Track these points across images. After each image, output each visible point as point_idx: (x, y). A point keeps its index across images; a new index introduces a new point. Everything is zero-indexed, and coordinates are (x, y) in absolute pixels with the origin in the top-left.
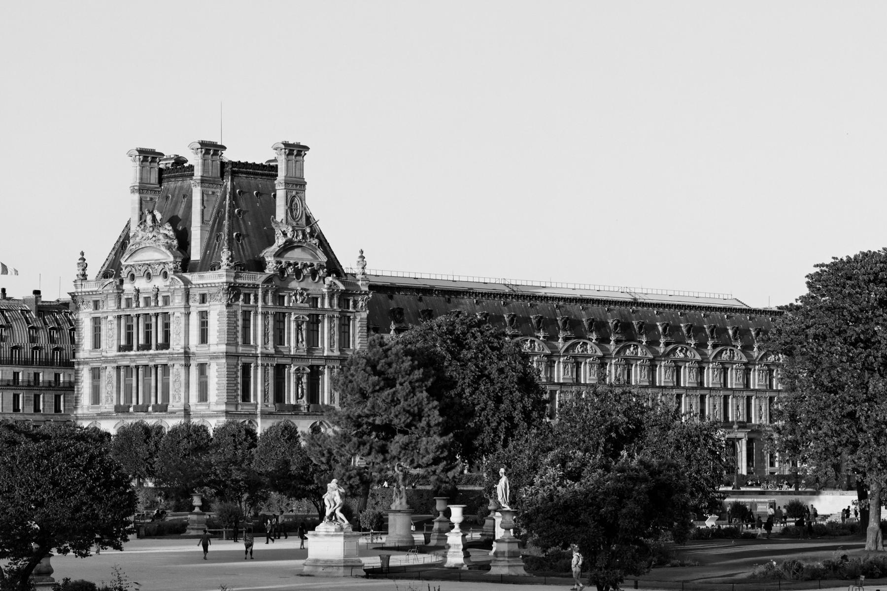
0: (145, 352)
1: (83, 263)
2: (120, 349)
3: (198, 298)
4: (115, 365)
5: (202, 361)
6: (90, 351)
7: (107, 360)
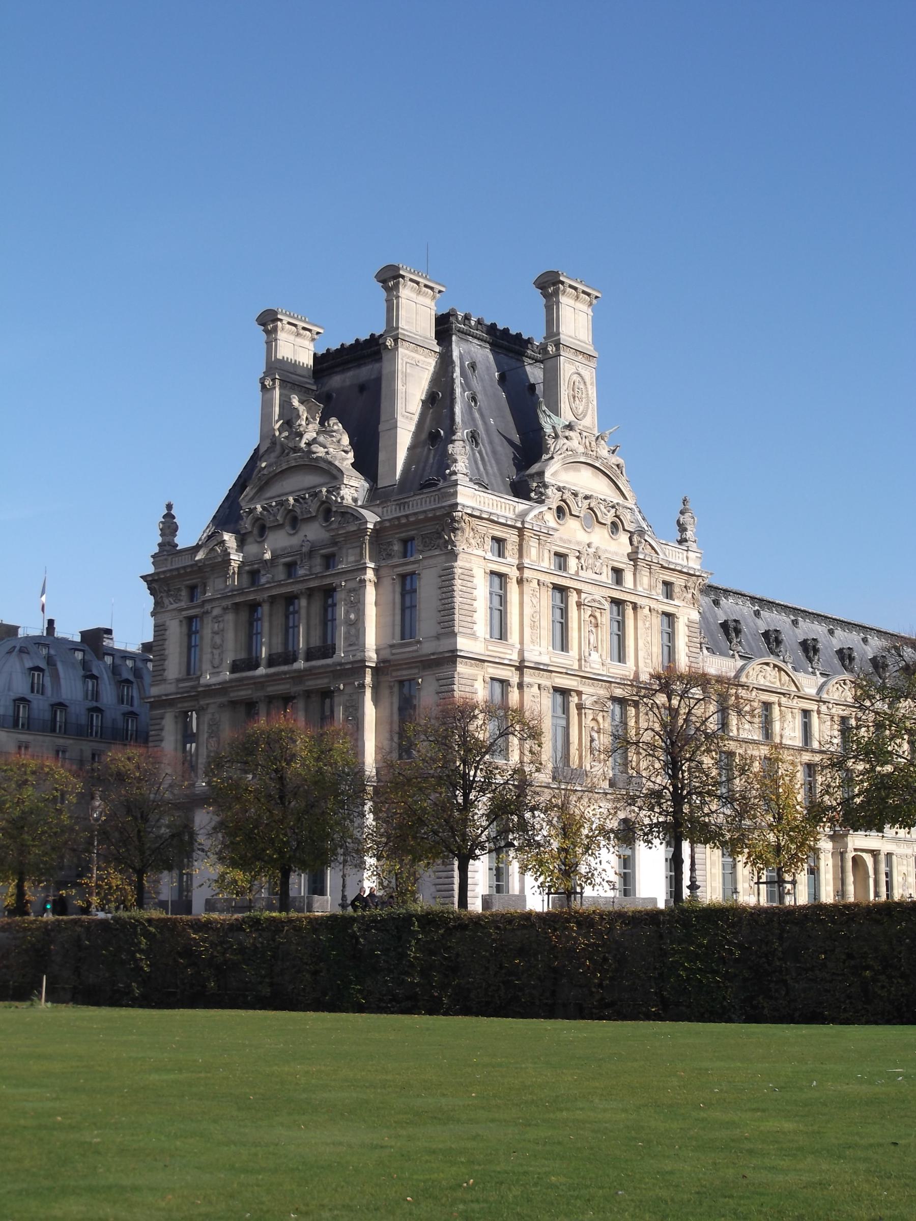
0: (285, 668)
1: (169, 526)
2: (235, 668)
3: (397, 547)
4: (223, 700)
5: (405, 674)
6: (178, 681)
7: (211, 691)
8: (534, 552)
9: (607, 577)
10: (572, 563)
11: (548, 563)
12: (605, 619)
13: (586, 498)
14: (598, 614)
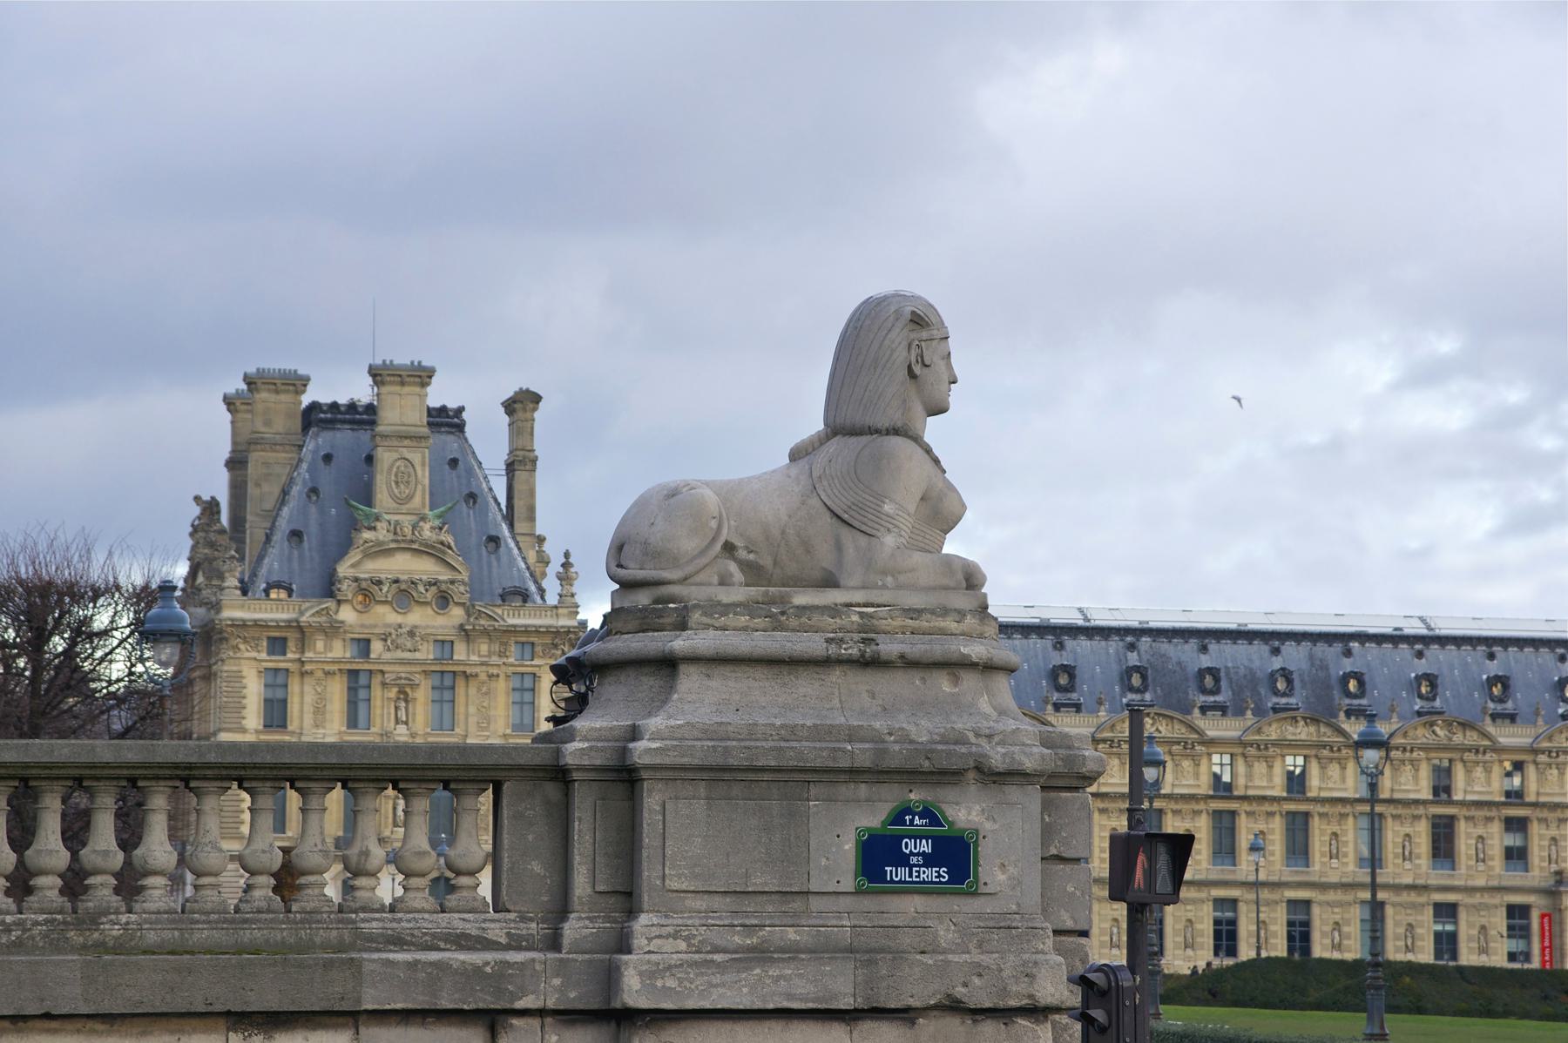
8: (320, 645)
9: (427, 652)
10: (377, 647)
11: (340, 650)
12: (423, 694)
13: (396, 581)
14: (408, 690)
